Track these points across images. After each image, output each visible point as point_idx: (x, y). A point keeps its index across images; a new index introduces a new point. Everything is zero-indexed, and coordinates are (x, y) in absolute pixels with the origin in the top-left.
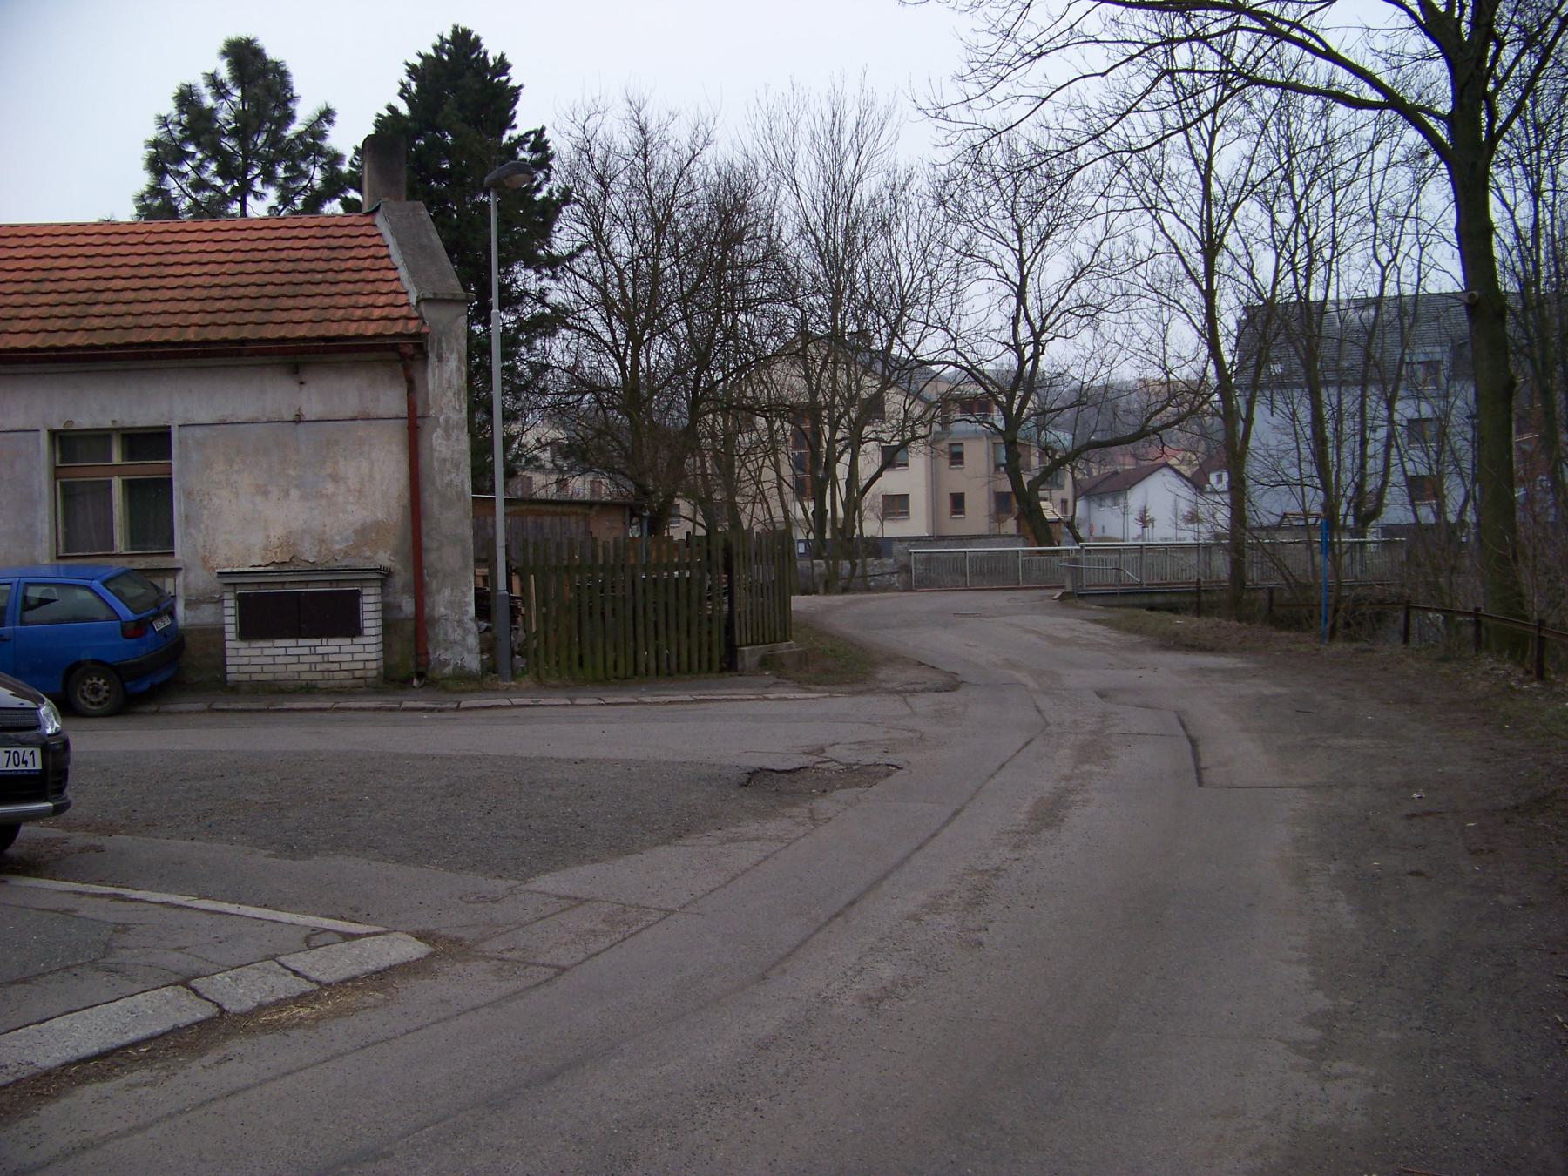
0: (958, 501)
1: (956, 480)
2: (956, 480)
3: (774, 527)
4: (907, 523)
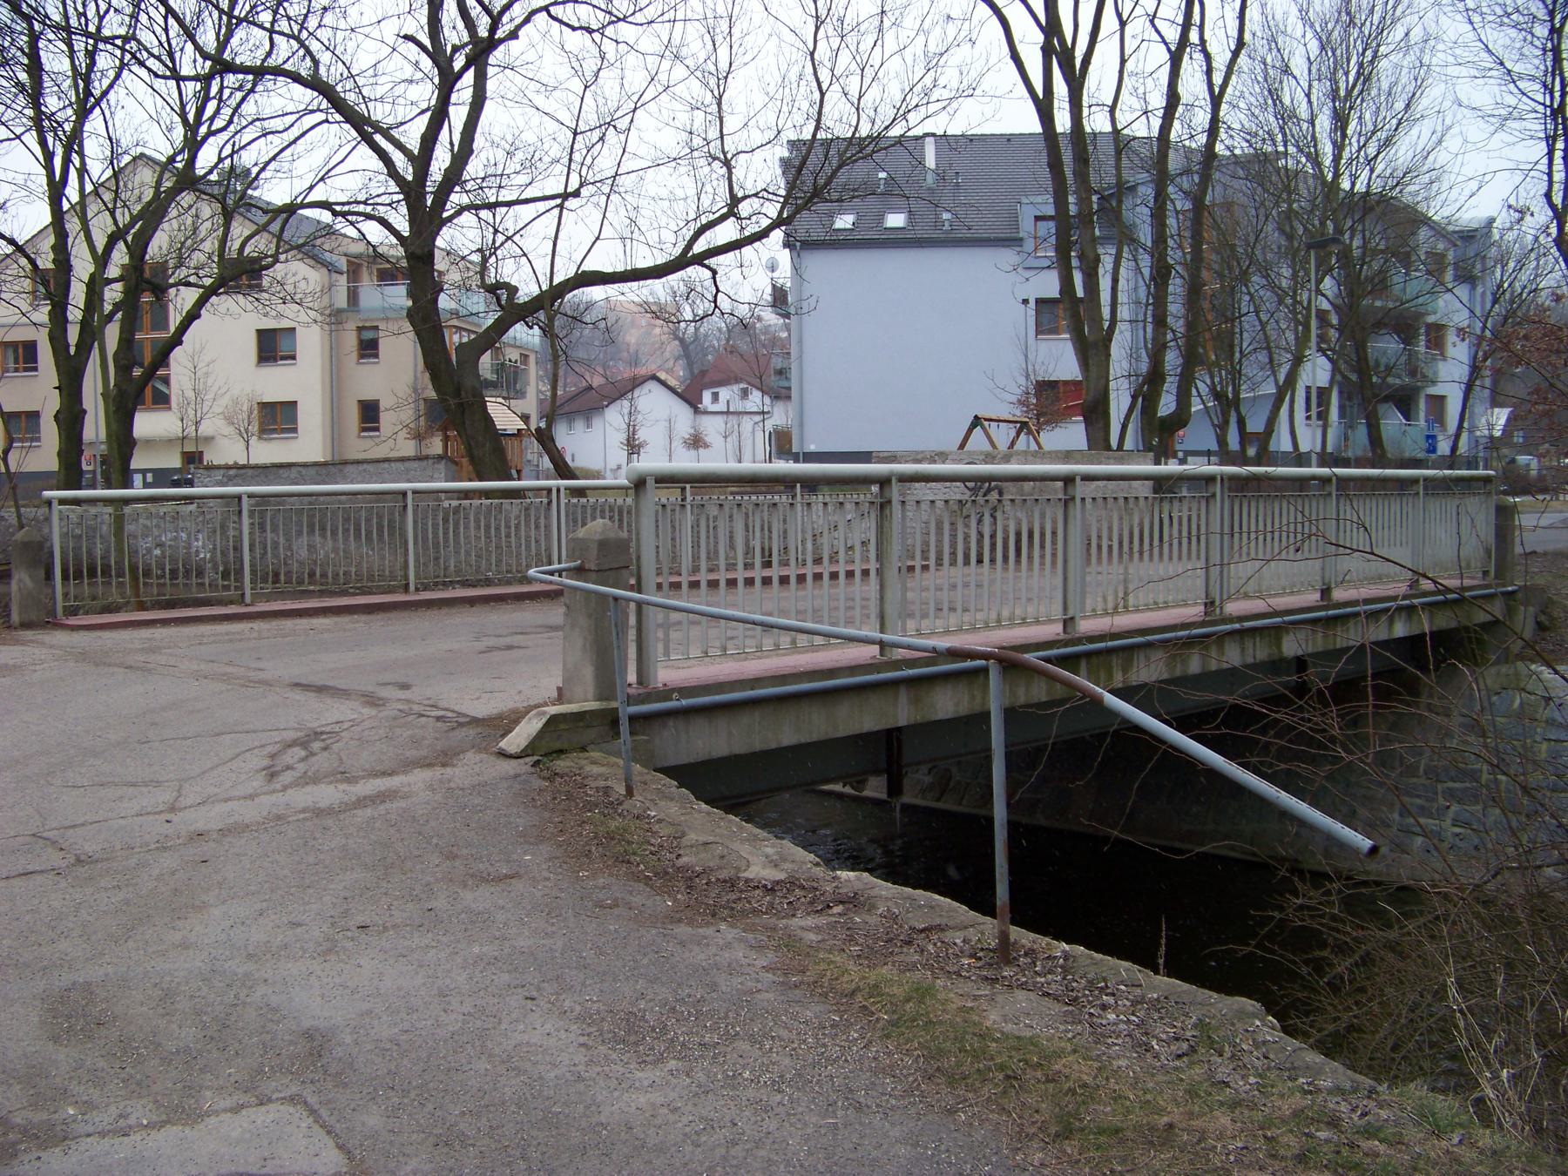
0: (370, 413)
1: (372, 381)
2: (372, 381)
3: (172, 286)
4: (293, 445)
